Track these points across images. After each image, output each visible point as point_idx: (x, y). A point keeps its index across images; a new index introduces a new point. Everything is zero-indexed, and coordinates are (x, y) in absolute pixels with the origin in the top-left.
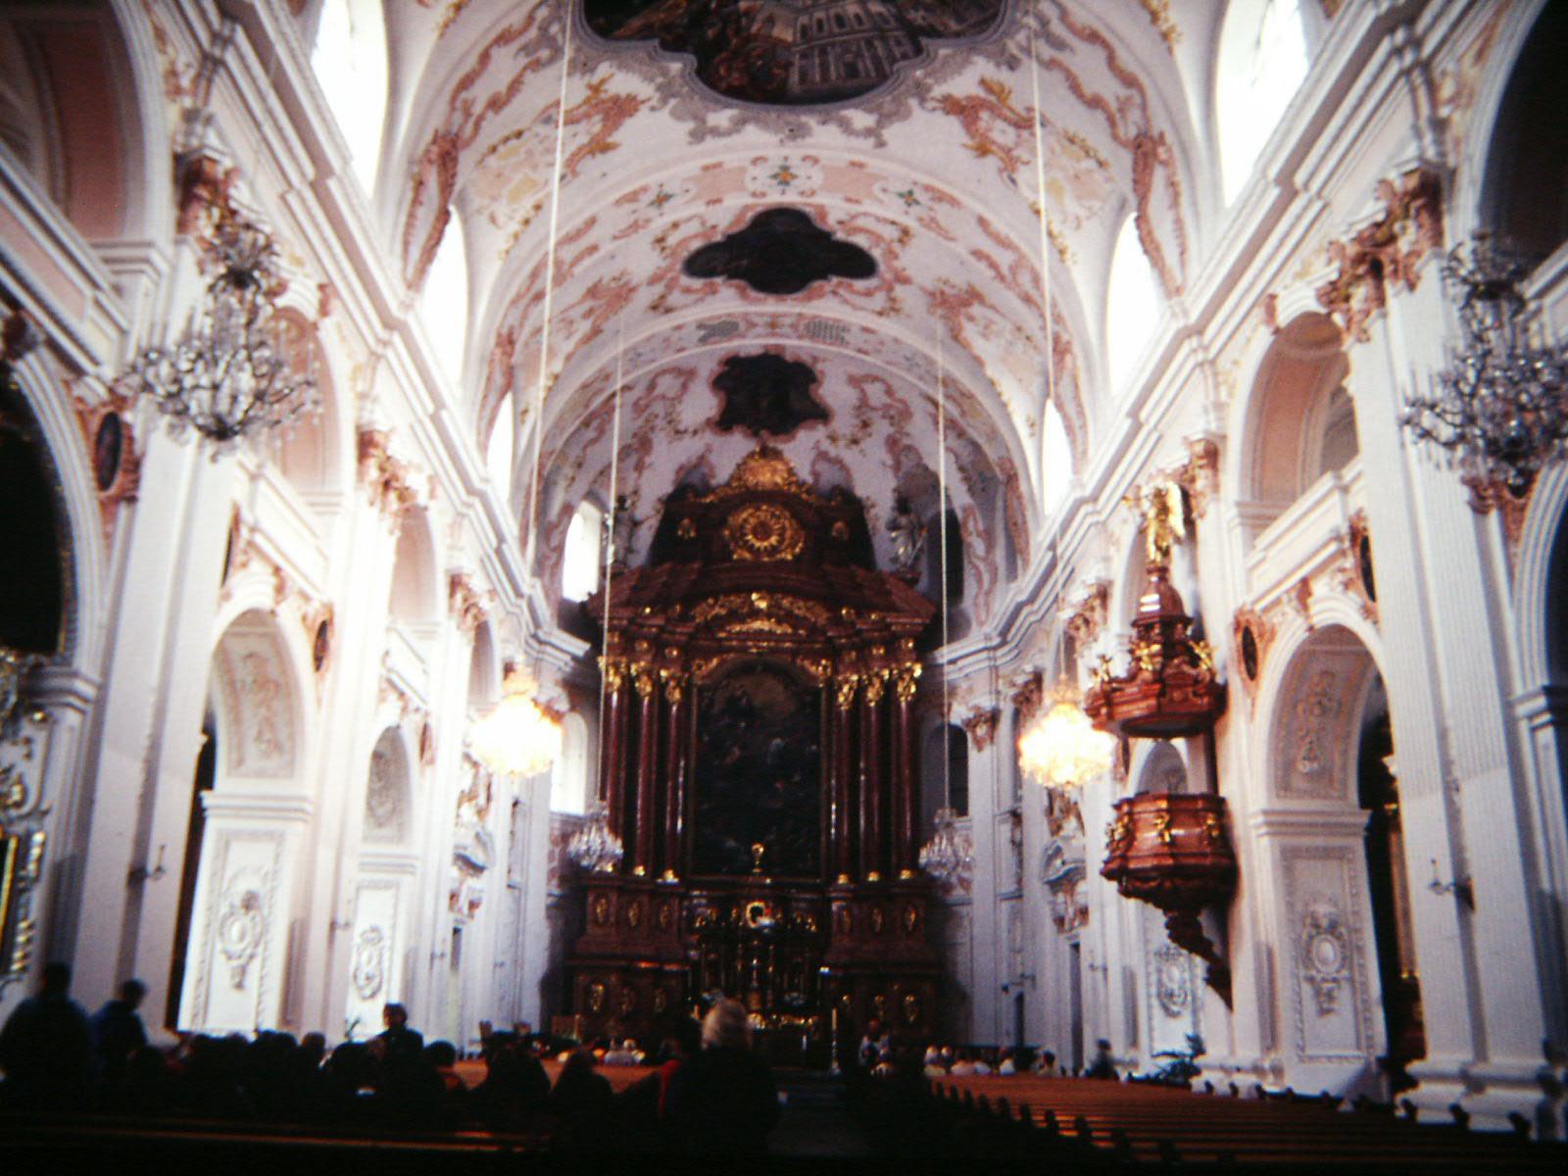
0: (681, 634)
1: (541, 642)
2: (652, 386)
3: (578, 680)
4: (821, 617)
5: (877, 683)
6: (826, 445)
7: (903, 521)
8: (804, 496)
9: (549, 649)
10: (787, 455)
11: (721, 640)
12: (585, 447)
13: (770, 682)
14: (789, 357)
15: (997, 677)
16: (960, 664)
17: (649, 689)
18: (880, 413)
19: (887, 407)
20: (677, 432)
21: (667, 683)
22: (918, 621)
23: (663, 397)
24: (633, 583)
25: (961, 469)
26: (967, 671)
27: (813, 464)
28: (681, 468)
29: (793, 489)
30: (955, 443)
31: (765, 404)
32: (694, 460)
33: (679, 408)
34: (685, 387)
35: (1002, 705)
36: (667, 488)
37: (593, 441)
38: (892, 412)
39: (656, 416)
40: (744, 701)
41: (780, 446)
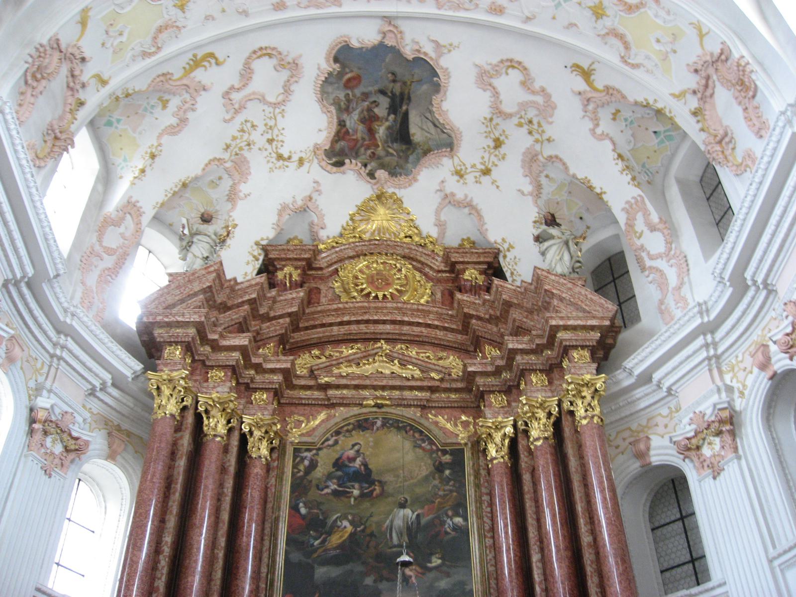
0: (273, 371)
1: (59, 332)
2: (247, 73)
3: (126, 426)
4: (453, 363)
5: (541, 414)
6: (453, 185)
7: (553, 231)
8: (430, 247)
9: (71, 344)
10: (406, 204)
11: (326, 387)
12: (160, 136)
13: (394, 439)
14: (408, 52)
15: (721, 372)
16: (656, 376)
17: (222, 430)
18: (515, 120)
19: (524, 106)
20: (280, 157)
21: (251, 432)
22: (594, 322)
23: (262, 100)
24: (208, 284)
25: (620, 156)
26: (666, 384)
27: (438, 212)
28: (284, 208)
29: (417, 239)
30: (606, 125)
31: (381, 131)
32: (300, 203)
33: (281, 123)
34: (287, 90)
35: (739, 405)
36: (267, 233)
37: (173, 131)
38: (531, 113)
39: (253, 126)
40: (358, 461)
41: (400, 193)
